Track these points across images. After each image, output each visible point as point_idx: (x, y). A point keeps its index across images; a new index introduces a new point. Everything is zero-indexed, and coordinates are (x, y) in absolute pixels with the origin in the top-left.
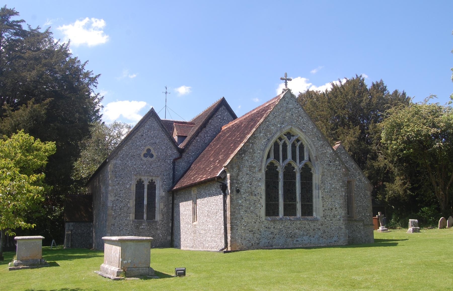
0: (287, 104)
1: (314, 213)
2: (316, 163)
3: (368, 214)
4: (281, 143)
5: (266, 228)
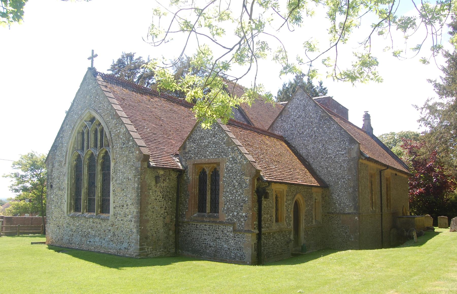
3: (244, 214)
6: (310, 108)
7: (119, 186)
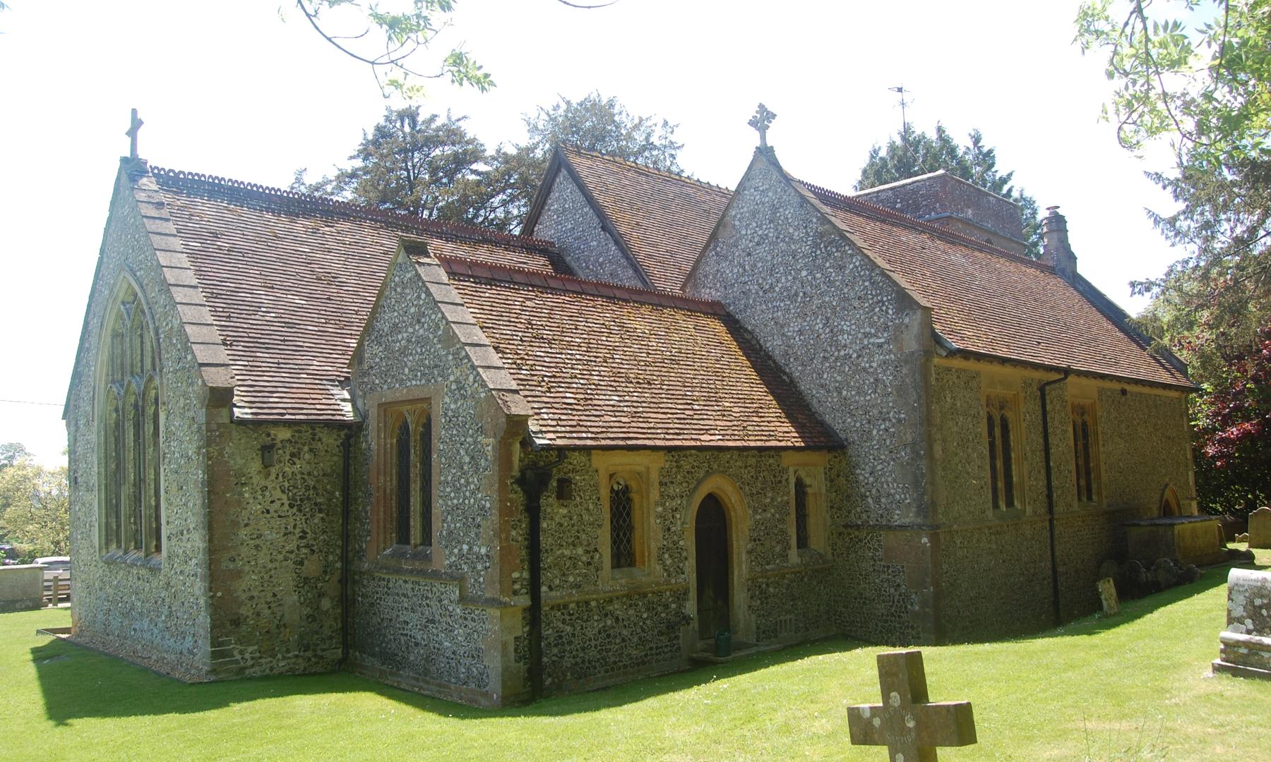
3: (483, 551)
6: (789, 212)
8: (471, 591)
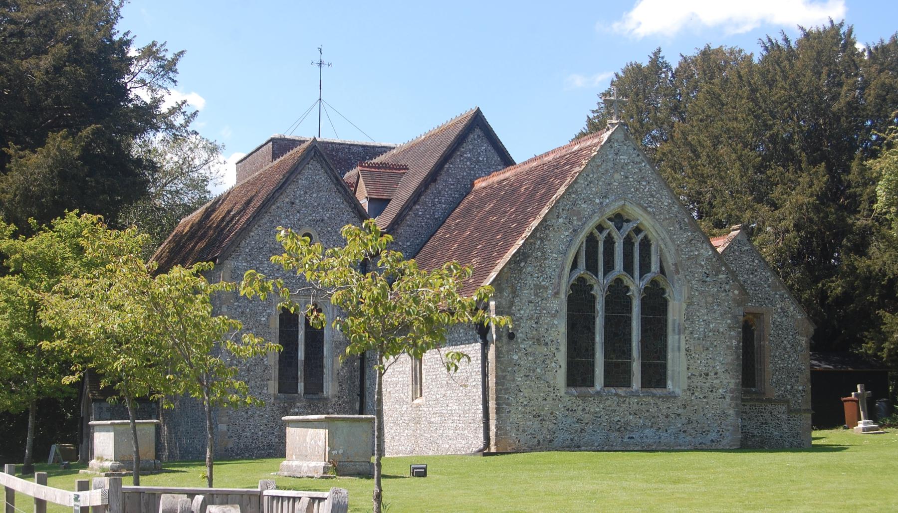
0: (616, 154)
1: (669, 383)
2: (676, 277)
3: (801, 388)
4: (601, 238)
5: (568, 410)
7: (698, 342)
8: (792, 407)
